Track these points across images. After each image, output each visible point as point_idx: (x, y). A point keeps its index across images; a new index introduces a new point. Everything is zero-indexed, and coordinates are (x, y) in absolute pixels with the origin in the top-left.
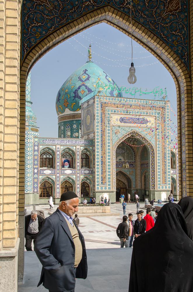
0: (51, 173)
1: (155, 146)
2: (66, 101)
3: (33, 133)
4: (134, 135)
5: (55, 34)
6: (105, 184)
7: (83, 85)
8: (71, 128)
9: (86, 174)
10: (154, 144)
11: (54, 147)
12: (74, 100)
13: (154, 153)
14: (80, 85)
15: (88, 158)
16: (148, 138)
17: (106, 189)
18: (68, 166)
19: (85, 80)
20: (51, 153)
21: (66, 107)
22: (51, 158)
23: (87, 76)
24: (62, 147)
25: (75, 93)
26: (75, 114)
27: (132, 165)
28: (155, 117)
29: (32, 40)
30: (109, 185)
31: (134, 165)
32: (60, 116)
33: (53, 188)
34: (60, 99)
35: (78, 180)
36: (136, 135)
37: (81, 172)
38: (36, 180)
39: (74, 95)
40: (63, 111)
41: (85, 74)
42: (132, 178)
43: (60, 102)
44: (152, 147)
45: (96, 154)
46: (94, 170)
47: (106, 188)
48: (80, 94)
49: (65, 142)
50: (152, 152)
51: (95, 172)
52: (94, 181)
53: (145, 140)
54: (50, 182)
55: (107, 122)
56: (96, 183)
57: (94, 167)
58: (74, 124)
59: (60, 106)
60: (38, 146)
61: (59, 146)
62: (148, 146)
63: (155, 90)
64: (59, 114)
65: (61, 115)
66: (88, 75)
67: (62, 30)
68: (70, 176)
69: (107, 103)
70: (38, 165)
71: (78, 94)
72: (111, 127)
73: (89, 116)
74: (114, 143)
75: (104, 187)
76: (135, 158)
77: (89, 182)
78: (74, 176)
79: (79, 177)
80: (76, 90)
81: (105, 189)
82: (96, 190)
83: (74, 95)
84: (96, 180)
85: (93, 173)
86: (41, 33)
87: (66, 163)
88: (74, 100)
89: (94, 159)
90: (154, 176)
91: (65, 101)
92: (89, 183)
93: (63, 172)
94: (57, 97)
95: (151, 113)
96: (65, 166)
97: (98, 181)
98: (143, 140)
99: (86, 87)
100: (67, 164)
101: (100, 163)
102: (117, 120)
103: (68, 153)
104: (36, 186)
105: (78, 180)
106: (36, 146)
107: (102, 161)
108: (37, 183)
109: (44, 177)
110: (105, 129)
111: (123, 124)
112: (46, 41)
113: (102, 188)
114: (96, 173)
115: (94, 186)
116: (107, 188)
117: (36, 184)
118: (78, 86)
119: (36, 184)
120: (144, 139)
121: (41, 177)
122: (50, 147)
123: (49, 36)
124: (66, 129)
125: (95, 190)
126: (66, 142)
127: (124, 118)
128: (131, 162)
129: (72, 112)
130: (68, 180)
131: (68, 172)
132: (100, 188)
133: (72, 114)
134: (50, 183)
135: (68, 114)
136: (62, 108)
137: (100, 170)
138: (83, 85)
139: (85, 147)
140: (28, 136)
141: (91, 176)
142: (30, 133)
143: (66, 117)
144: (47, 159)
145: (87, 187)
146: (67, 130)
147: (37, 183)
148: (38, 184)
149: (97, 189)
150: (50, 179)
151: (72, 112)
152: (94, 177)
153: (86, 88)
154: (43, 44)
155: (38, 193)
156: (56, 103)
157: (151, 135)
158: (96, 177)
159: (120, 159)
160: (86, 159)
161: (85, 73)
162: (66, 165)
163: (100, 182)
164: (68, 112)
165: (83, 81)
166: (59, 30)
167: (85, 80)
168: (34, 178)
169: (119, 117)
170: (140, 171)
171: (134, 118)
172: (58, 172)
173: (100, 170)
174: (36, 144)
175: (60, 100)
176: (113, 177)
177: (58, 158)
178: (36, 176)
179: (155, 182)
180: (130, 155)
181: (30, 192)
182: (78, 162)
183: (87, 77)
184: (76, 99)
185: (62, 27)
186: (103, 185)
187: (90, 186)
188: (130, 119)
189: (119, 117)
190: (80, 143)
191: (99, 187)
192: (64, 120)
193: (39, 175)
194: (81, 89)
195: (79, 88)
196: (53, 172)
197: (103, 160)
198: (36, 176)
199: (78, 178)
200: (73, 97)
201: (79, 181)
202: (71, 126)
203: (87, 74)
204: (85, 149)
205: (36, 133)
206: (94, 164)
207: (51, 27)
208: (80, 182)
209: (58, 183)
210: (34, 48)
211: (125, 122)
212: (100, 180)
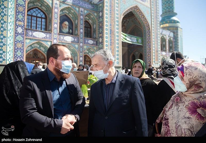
0: (44, 38)
9: (90, 44)
35: (81, 51)
38: (19, 45)
50: (148, 31)
53: (143, 18)
70: (24, 22)
78: (77, 46)
79: (82, 47)
105: (81, 51)
107: (111, 30)
108: (21, 49)
117: (19, 52)
119: (19, 52)
137: (109, 40)
147: (21, 49)
148: (23, 52)
168: (15, 41)
177: (56, 17)
178: (19, 38)
179: (151, 60)
182: (81, 29)
193: (25, 37)
197: (112, 29)
199: (81, 49)
201: (82, 52)
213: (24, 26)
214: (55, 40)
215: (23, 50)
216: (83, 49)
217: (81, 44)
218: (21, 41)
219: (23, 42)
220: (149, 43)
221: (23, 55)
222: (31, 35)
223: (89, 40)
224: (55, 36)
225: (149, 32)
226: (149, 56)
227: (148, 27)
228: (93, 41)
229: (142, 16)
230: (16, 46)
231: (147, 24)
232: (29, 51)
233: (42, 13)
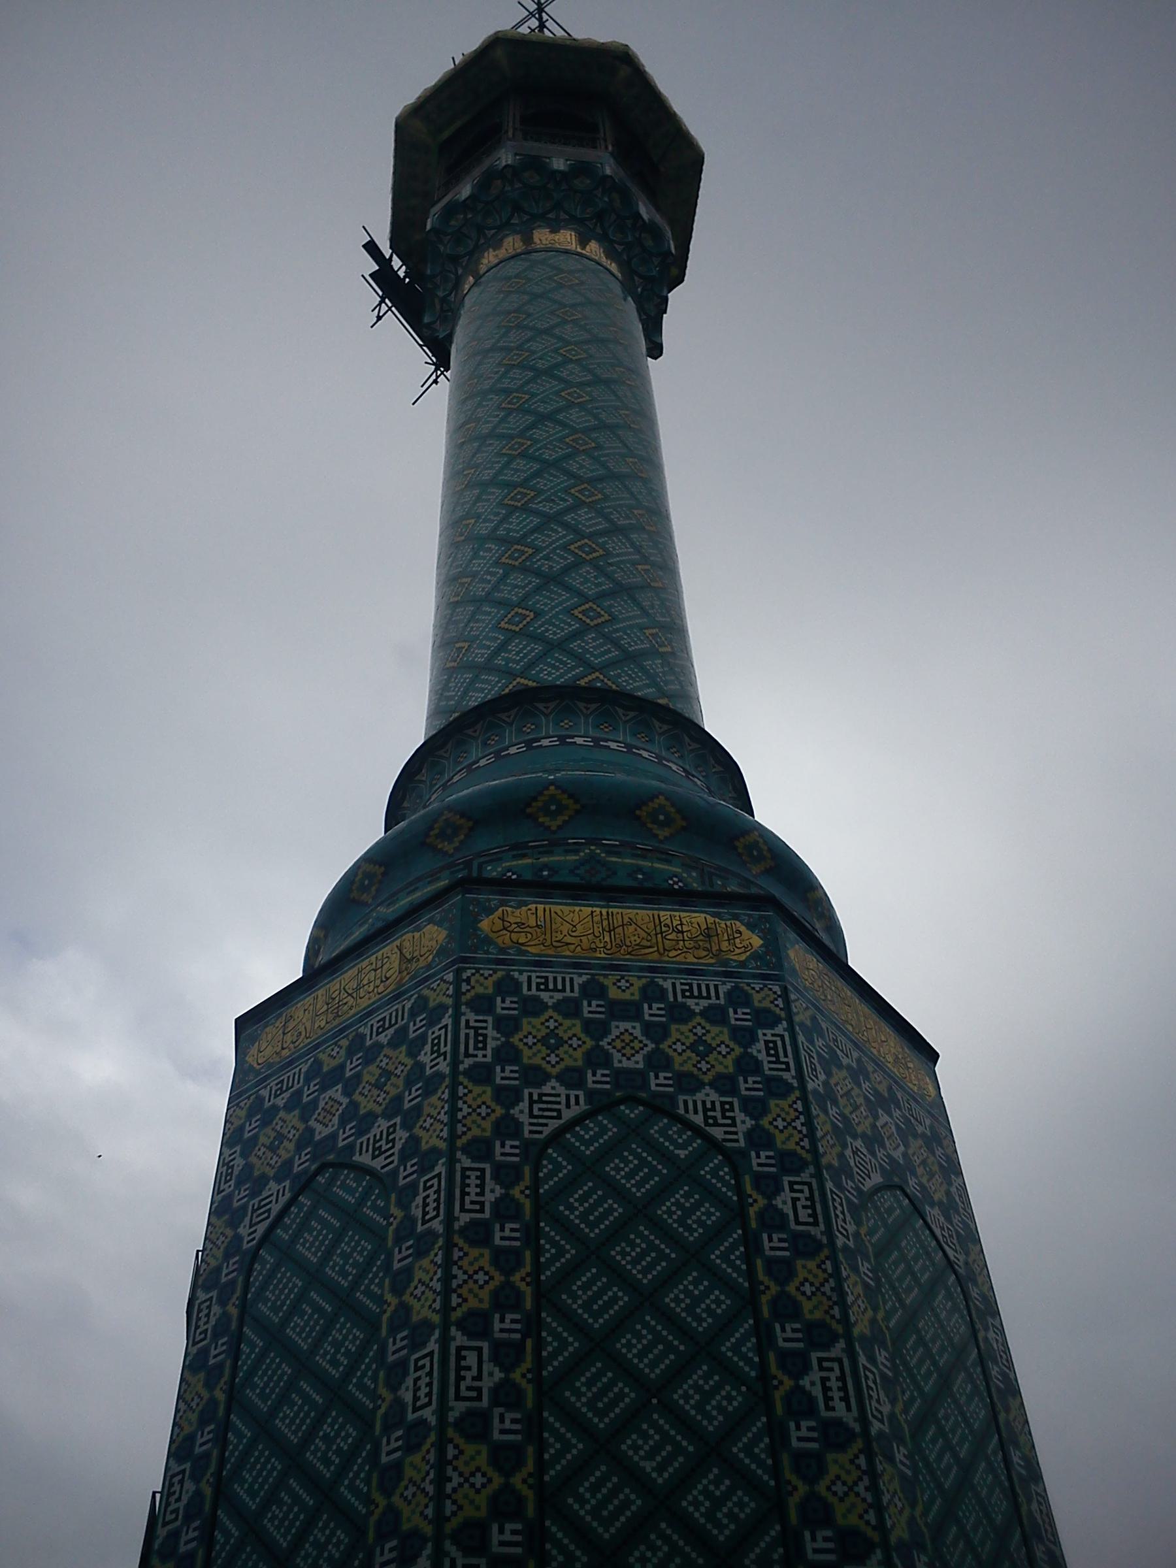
140: (758, 1050)
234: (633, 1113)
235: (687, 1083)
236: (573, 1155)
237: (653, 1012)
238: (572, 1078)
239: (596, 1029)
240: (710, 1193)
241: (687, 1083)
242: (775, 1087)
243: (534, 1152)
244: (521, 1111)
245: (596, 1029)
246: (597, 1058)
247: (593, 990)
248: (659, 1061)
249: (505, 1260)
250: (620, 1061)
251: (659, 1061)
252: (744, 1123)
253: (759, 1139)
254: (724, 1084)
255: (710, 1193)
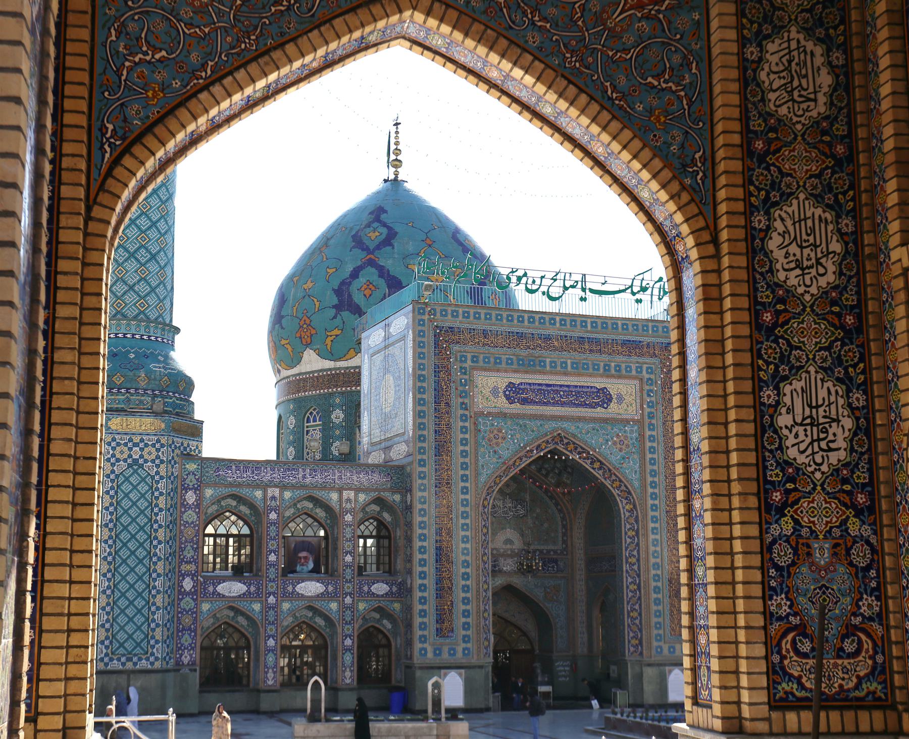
1: (639, 491)
2: (308, 322)
3: (180, 440)
4: (560, 448)
5: (216, 89)
6: (450, 634)
7: (371, 263)
8: (324, 424)
9: (378, 596)
10: (636, 484)
11: (259, 494)
12: (335, 317)
13: (637, 517)
14: (359, 263)
15: (384, 537)
16: (612, 456)
17: (454, 654)
18: (311, 565)
19: (378, 247)
20: (245, 515)
21: (307, 345)
22: (245, 536)
23: (384, 231)
24: (287, 495)
25: (338, 292)
26: (339, 369)
27: (555, 561)
28: (637, 382)
29: (131, 111)
30: (464, 641)
31: (561, 564)
32: (282, 376)
33: (252, 649)
34: (283, 313)
35: (348, 619)
36: (567, 449)
37: (360, 588)
38: (187, 620)
39: (335, 301)
40: (296, 360)
41: (376, 225)
42: (556, 611)
43: (282, 328)
44: (629, 493)
45: (417, 519)
46: (409, 582)
47: (454, 649)
48: (358, 298)
49: (300, 476)
50: (627, 514)
51: (410, 591)
52: (409, 625)
53: (600, 468)
54: (242, 626)
55: (455, 401)
56: (418, 633)
57: (410, 572)
58: (334, 406)
59: (283, 342)
60: (198, 489)
61: (277, 492)
62: (615, 492)
63: (637, 283)
64: (279, 371)
65: (285, 373)
66: (389, 228)
67: (241, 75)
68: (318, 605)
69: (456, 330)
71: (350, 296)
72: (472, 420)
73: (390, 378)
74: (483, 479)
75: (446, 649)
76: (564, 534)
77: (389, 626)
78: (334, 606)
80: (343, 283)
81: (450, 654)
82: (417, 660)
83: (335, 301)
84: (417, 620)
85: (403, 592)
86: (164, 87)
87: (303, 554)
88: (335, 317)
89: (409, 540)
90: (637, 607)
91: (303, 322)
92: (389, 630)
93: (290, 588)
94: (273, 309)
95: (623, 366)
96: (298, 568)
97: (425, 623)
98: (593, 468)
99: (383, 272)
100: (305, 558)
101: (430, 556)
102: (495, 391)
103: (310, 516)
104: (186, 644)
105: (348, 619)
106: (190, 489)
108: (190, 629)
109: (219, 604)
110: (449, 426)
111: (516, 408)
112: (183, 113)
113: (437, 652)
114: (418, 594)
115: (409, 643)
116: (460, 649)
117: (186, 636)
118: (349, 268)
119: (186, 636)
120: (597, 465)
121: (205, 607)
122: (244, 492)
123: (194, 95)
124: (306, 425)
125: (411, 658)
126: (304, 477)
127: (522, 387)
128: (549, 551)
129: (328, 364)
130: (311, 618)
131: (311, 588)
132: (430, 650)
133: (330, 369)
134: (243, 630)
135: (313, 372)
136: (290, 349)
137: (430, 582)
138: (371, 263)
139: (374, 495)
140: (160, 453)
141: (397, 606)
142: (170, 442)
143: (304, 380)
144: (231, 540)
145: (384, 646)
146: (308, 432)
149: (421, 654)
150: (243, 614)
151: (328, 364)
152: (408, 609)
153: (381, 276)
154: (172, 123)
155: (195, 670)
156: (271, 332)
157: (624, 447)
158: (418, 607)
159: (508, 541)
160: (378, 538)
161: (377, 219)
162: (303, 561)
163: (433, 626)
164: (312, 362)
165: (371, 248)
166: (230, 73)
167: (378, 247)
168: (179, 612)
169: (501, 381)
170: (584, 587)
171: (561, 386)
172: (272, 588)
173: (433, 582)
174: (191, 481)
175: (284, 321)
176: (482, 608)
180: (546, 525)
181: (165, 666)
183: (384, 236)
184: (343, 313)
185: (244, 65)
186: (441, 640)
187: (393, 644)
188: (544, 388)
189: (501, 381)
190: (355, 478)
191: (425, 645)
192: (299, 392)
193: (199, 599)
194: (361, 280)
195: (355, 274)
196: (253, 589)
198: (187, 603)
199: (348, 612)
200: (334, 307)
201: (350, 623)
202: (326, 416)
203: (385, 225)
204: (378, 501)
205: (191, 443)
206: (409, 559)
207: (204, 67)
208: (357, 627)
209: (271, 629)
210: (139, 139)
211: (524, 401)
212: (431, 620)
213: (197, 572)
214: (272, 597)
215: (195, 631)
216: (353, 612)
217: (348, 600)
218: (190, 610)
219: (195, 613)
220: (633, 565)
221: (195, 644)
222: (213, 593)
223: (374, 583)
224: (272, 587)
225: (632, 520)
226: (635, 614)
227: (626, 499)
228: (387, 584)
229: (592, 463)
230: (180, 624)
231: (623, 488)
232: (209, 628)
233: (241, 523)
234: (135, 467)
235: (146, 461)
236: (124, 476)
237: (141, 445)
238: (125, 460)
239: (130, 449)
240: (147, 484)
241: (146, 461)
242: (162, 462)
243: (117, 476)
244: (115, 468)
245: (130, 449)
246: (130, 456)
247: (131, 440)
248: (141, 456)
249: (112, 497)
250: (134, 457)
251: (141, 456)
252: (155, 469)
253: (157, 473)
254: (153, 461)
255: (147, 484)
